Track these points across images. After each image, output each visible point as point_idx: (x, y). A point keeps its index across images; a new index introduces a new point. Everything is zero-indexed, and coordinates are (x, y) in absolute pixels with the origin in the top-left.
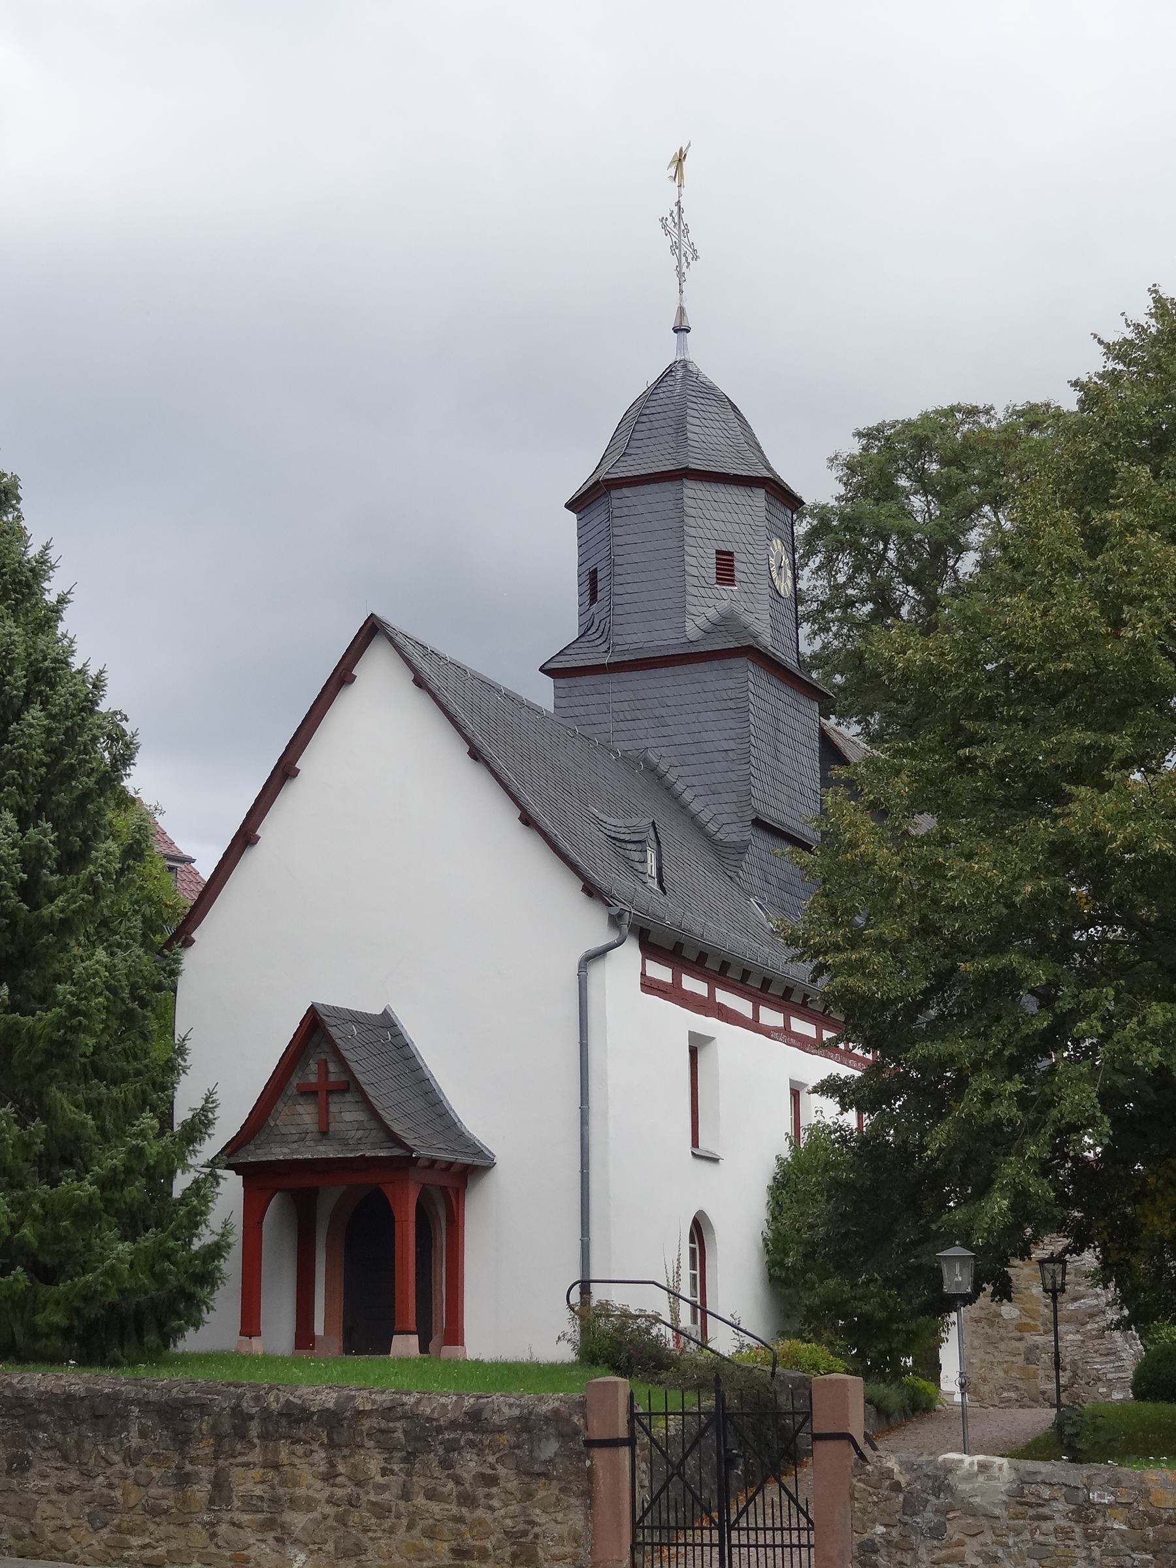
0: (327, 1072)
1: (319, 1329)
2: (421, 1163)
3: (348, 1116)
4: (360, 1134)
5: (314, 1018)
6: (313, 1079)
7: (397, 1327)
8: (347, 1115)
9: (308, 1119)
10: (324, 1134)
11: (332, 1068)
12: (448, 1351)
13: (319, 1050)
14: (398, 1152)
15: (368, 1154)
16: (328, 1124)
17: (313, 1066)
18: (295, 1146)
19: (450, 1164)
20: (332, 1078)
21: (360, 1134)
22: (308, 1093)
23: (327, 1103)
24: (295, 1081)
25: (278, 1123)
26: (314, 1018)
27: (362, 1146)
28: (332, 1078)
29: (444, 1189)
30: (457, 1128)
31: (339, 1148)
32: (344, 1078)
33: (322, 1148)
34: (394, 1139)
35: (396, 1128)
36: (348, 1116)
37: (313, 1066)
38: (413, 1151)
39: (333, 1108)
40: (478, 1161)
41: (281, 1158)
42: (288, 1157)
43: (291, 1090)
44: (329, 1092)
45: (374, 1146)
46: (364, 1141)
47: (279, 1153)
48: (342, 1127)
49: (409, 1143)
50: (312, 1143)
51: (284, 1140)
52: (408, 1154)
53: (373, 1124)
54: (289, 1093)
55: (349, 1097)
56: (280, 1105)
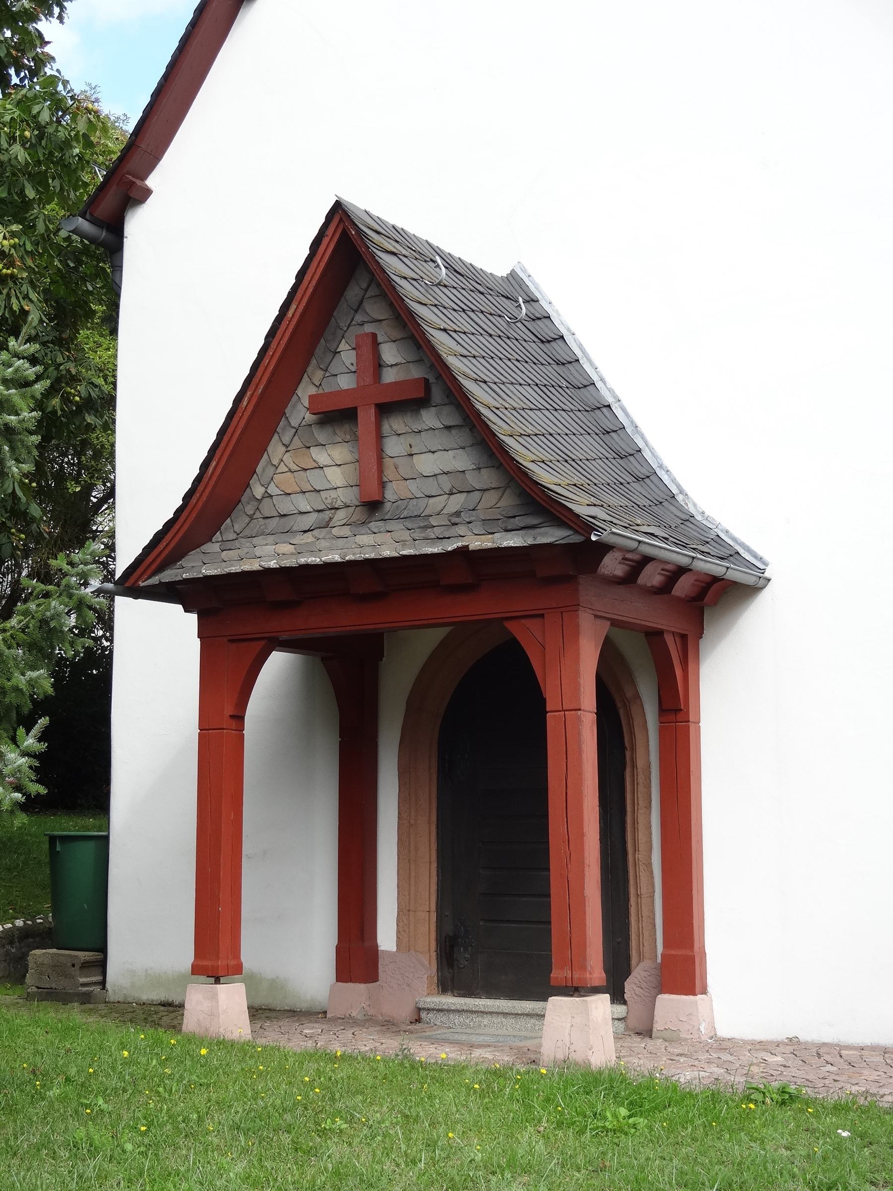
0: (379, 365)
1: (386, 937)
2: (611, 565)
3: (427, 464)
4: (456, 502)
5: (345, 235)
6: (346, 382)
7: (558, 974)
8: (426, 458)
9: (336, 476)
10: (372, 507)
11: (390, 353)
12: (669, 1006)
13: (359, 318)
14: (551, 535)
15: (475, 544)
16: (382, 485)
17: (347, 356)
18: (309, 538)
19: (681, 570)
20: (390, 376)
21: (456, 502)
22: (336, 416)
23: (380, 437)
24: (305, 391)
25: (273, 490)
26: (345, 235)
27: (461, 530)
28: (390, 376)
29: (654, 636)
30: (680, 508)
31: (406, 535)
32: (416, 373)
33: (365, 539)
34: (539, 503)
35: (544, 477)
36: (427, 464)
37: (347, 356)
38: (589, 528)
39: (394, 447)
40: (736, 574)
41: (273, 564)
42: (287, 563)
43: (299, 412)
44: (385, 410)
45: (490, 525)
46: (465, 517)
47: (269, 554)
48: (413, 487)
49: (582, 510)
50: (346, 531)
51: (284, 525)
52: (577, 539)
53: (488, 478)
54: (295, 422)
55: (429, 418)
56: (275, 450)
